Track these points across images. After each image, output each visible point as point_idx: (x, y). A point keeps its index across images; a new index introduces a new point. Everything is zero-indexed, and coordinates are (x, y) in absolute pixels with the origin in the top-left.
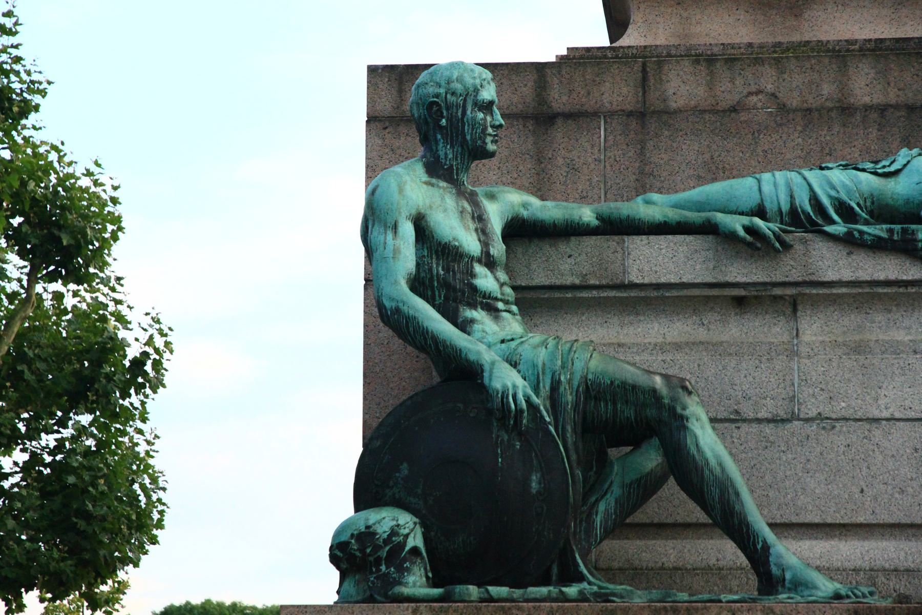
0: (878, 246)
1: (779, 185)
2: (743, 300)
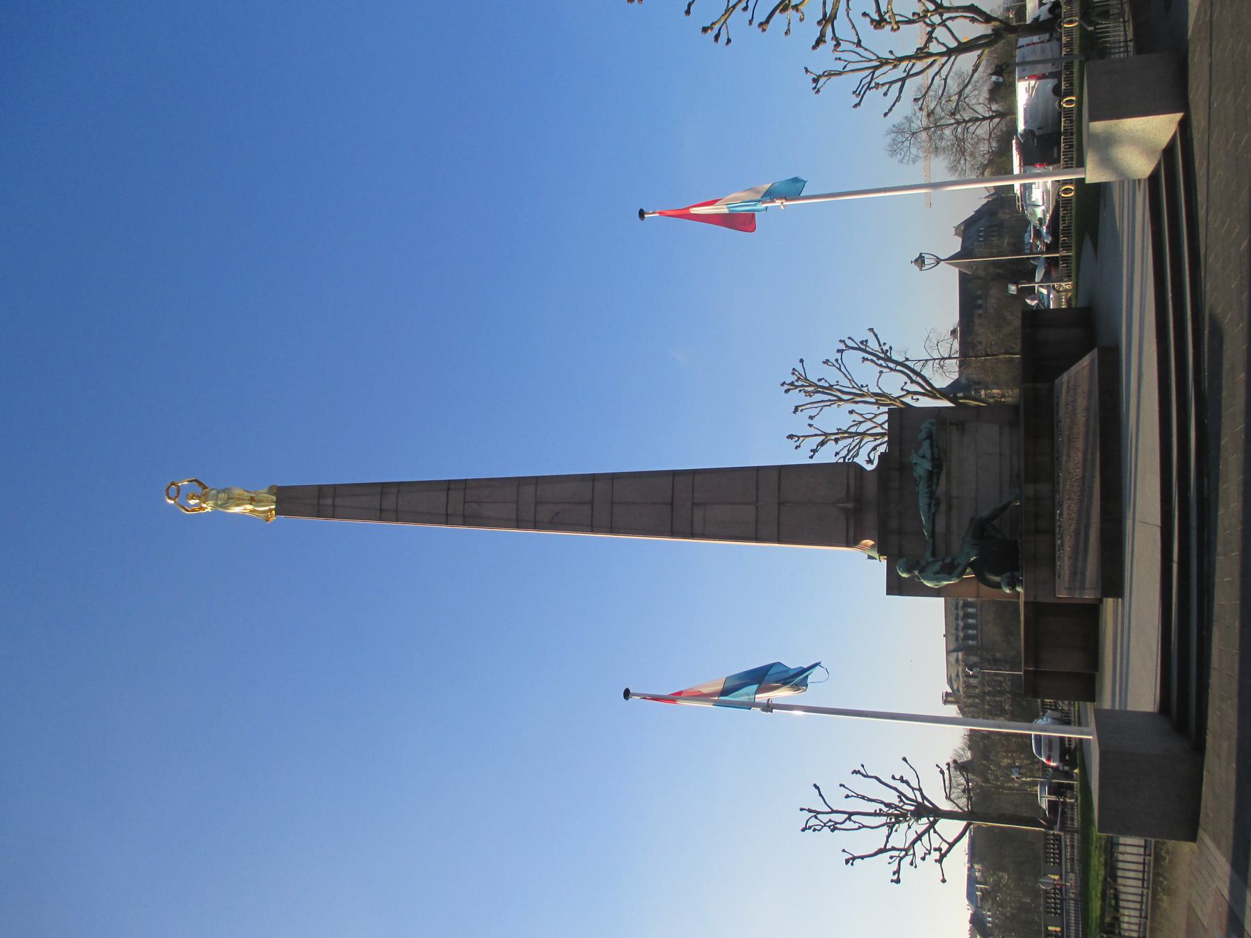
0: (938, 479)
1: (923, 502)
2: (950, 508)
